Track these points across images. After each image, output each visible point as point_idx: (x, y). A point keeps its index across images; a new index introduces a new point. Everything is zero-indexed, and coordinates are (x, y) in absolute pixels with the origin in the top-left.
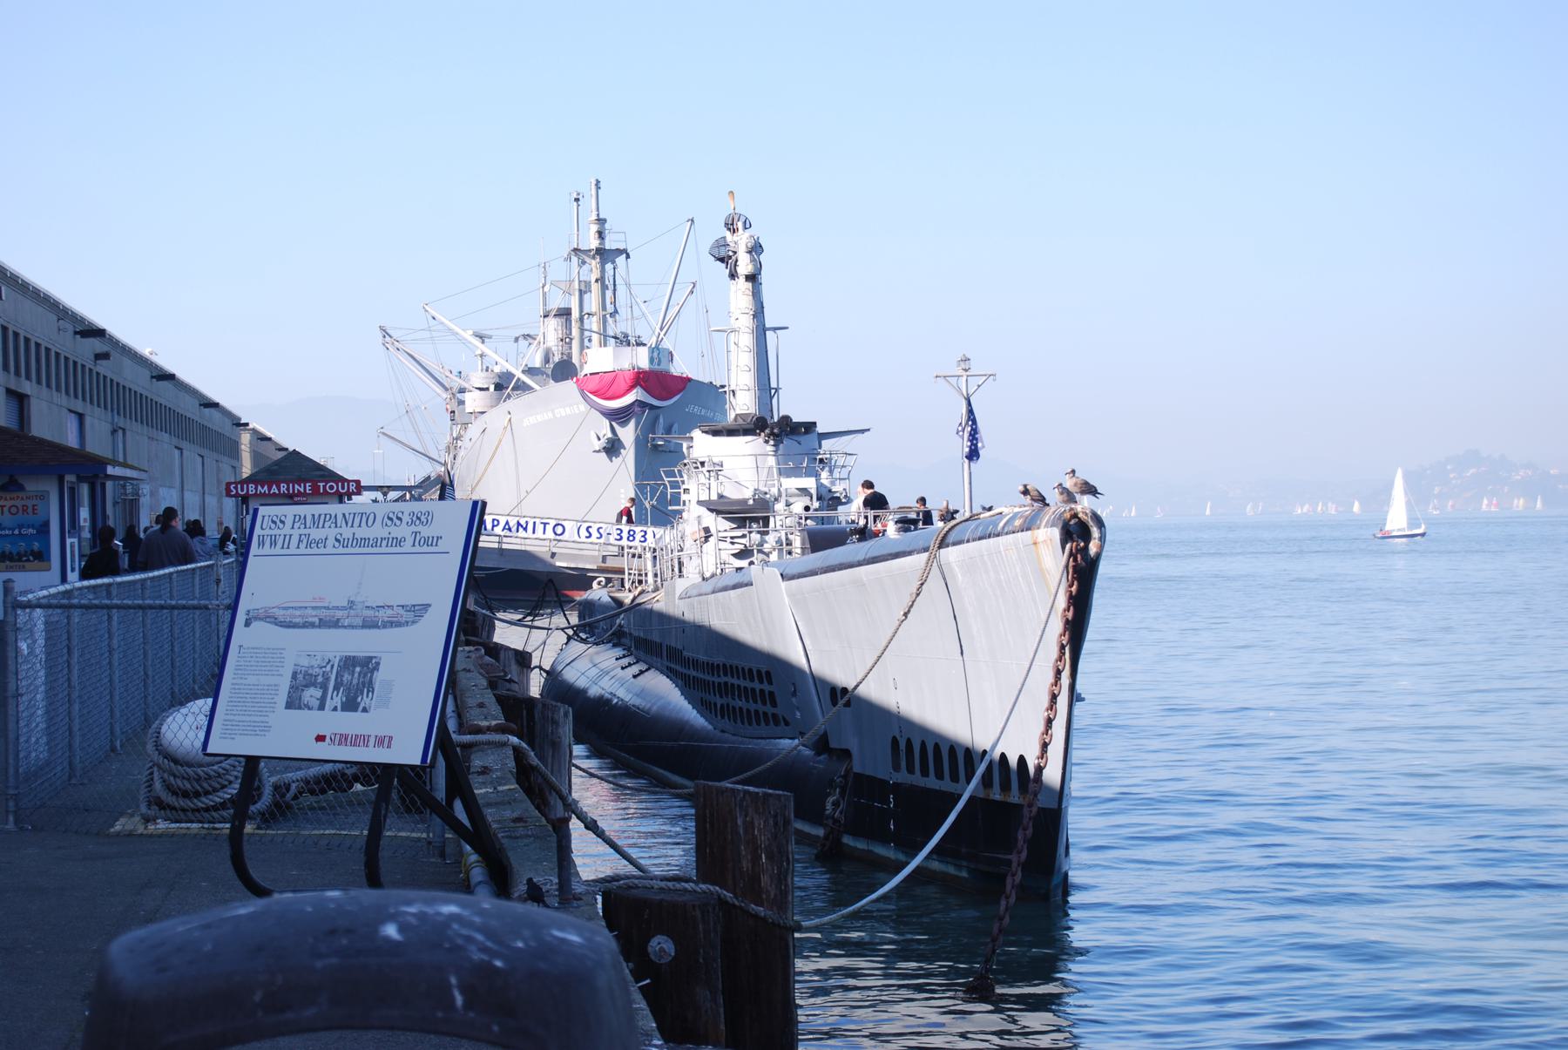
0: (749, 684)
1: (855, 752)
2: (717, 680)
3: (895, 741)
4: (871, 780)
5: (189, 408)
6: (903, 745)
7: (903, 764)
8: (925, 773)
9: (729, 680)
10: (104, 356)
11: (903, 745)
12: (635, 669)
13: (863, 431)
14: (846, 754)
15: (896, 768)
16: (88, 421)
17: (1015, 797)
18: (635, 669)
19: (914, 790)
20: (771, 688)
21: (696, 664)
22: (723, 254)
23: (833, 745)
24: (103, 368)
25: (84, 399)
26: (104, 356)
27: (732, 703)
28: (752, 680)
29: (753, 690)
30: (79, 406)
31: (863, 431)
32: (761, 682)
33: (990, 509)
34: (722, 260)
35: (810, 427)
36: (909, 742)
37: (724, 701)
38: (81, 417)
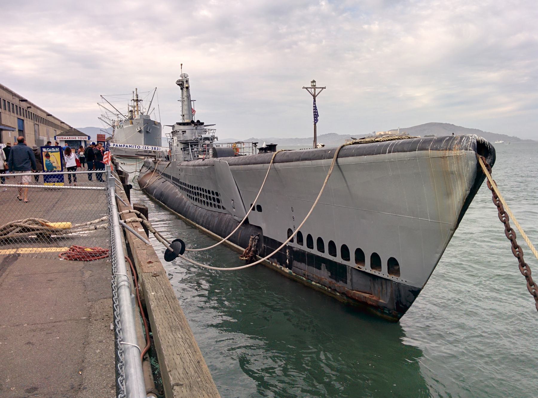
5: (44, 116)
7: (295, 240)
10: (30, 107)
12: (163, 180)
14: (259, 228)
16: (25, 121)
17: (383, 273)
18: (163, 180)
20: (218, 197)
23: (251, 222)
24: (30, 110)
25: (24, 116)
26: (30, 107)
30: (22, 118)
34: (179, 85)
35: (202, 124)
38: (23, 120)
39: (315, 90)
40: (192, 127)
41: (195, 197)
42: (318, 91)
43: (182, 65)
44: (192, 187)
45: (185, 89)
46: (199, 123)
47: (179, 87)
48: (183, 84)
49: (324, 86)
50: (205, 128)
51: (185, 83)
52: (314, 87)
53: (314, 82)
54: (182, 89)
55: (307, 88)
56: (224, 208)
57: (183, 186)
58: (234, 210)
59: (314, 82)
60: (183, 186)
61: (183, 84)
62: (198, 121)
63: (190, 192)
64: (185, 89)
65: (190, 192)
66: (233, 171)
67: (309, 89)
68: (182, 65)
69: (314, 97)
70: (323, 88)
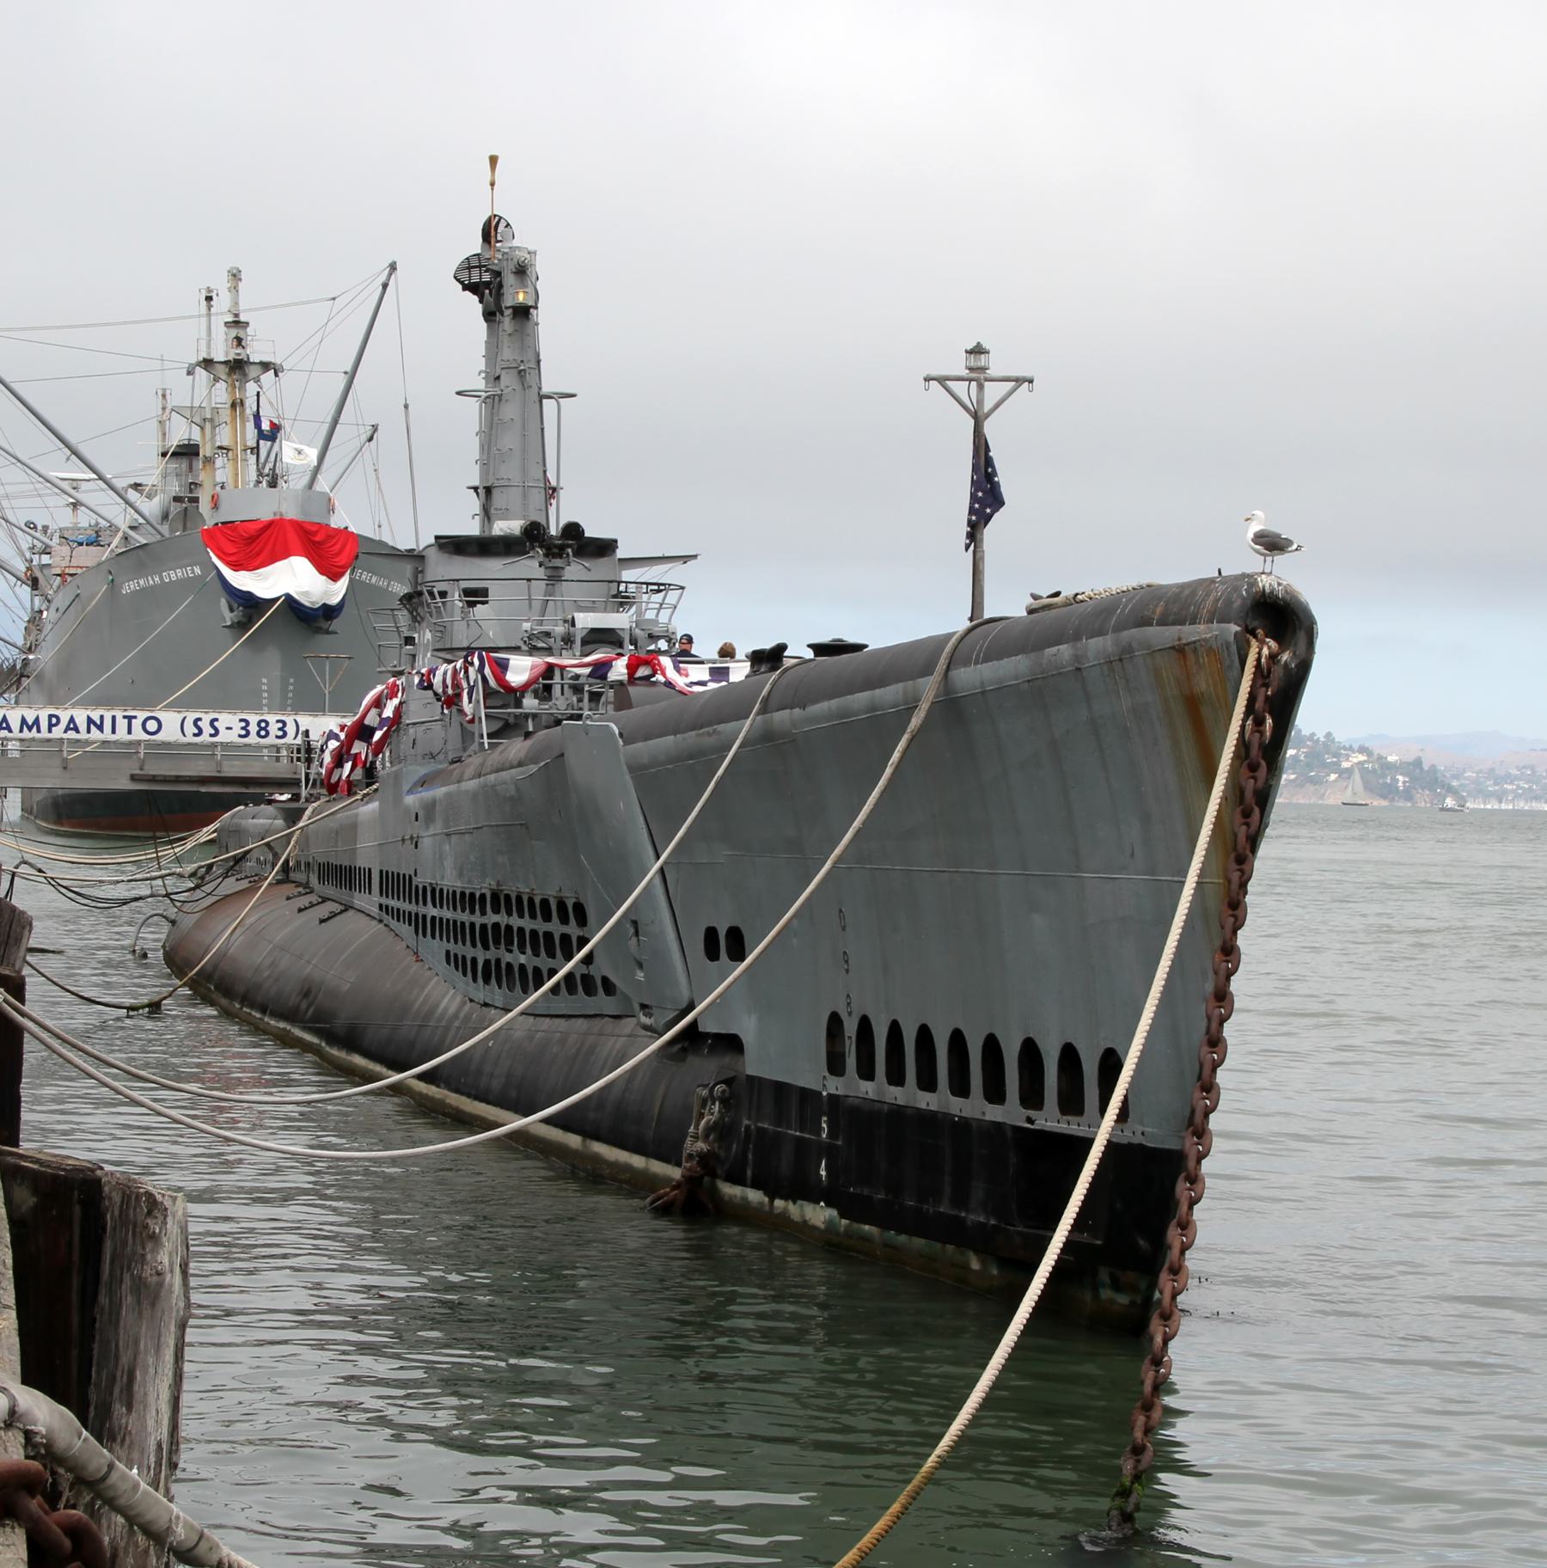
0: (541, 926)
1: (748, 1038)
2: (478, 919)
3: (835, 1022)
4: (781, 1089)
6: (851, 1028)
7: (851, 1062)
8: (896, 1077)
9: (502, 919)
11: (851, 1028)
13: (685, 559)
14: (732, 1043)
15: (835, 1065)
19: (899, 1115)
21: (436, 895)
22: (475, 279)
27: (507, 958)
28: (547, 917)
29: (549, 936)
31: (685, 559)
32: (564, 920)
33: (1057, 594)
36: (865, 1025)
37: (492, 954)
39: (981, 387)
40: (530, 566)
41: (481, 956)
42: (993, 392)
43: (493, 160)
44: (469, 901)
45: (507, 323)
46: (579, 544)
47: (472, 304)
48: (497, 284)
49: (1027, 374)
50: (628, 575)
51: (509, 280)
52: (978, 375)
53: (978, 351)
54: (490, 315)
55: (942, 380)
56: (609, 987)
57: (432, 911)
58: (640, 975)
59: (978, 351)
60: (432, 911)
61: (497, 284)
62: (573, 530)
63: (456, 931)
64: (507, 323)
65: (456, 931)
66: (636, 770)
67: (960, 388)
68: (493, 160)
69: (978, 419)
70: (1019, 381)
